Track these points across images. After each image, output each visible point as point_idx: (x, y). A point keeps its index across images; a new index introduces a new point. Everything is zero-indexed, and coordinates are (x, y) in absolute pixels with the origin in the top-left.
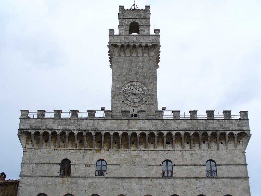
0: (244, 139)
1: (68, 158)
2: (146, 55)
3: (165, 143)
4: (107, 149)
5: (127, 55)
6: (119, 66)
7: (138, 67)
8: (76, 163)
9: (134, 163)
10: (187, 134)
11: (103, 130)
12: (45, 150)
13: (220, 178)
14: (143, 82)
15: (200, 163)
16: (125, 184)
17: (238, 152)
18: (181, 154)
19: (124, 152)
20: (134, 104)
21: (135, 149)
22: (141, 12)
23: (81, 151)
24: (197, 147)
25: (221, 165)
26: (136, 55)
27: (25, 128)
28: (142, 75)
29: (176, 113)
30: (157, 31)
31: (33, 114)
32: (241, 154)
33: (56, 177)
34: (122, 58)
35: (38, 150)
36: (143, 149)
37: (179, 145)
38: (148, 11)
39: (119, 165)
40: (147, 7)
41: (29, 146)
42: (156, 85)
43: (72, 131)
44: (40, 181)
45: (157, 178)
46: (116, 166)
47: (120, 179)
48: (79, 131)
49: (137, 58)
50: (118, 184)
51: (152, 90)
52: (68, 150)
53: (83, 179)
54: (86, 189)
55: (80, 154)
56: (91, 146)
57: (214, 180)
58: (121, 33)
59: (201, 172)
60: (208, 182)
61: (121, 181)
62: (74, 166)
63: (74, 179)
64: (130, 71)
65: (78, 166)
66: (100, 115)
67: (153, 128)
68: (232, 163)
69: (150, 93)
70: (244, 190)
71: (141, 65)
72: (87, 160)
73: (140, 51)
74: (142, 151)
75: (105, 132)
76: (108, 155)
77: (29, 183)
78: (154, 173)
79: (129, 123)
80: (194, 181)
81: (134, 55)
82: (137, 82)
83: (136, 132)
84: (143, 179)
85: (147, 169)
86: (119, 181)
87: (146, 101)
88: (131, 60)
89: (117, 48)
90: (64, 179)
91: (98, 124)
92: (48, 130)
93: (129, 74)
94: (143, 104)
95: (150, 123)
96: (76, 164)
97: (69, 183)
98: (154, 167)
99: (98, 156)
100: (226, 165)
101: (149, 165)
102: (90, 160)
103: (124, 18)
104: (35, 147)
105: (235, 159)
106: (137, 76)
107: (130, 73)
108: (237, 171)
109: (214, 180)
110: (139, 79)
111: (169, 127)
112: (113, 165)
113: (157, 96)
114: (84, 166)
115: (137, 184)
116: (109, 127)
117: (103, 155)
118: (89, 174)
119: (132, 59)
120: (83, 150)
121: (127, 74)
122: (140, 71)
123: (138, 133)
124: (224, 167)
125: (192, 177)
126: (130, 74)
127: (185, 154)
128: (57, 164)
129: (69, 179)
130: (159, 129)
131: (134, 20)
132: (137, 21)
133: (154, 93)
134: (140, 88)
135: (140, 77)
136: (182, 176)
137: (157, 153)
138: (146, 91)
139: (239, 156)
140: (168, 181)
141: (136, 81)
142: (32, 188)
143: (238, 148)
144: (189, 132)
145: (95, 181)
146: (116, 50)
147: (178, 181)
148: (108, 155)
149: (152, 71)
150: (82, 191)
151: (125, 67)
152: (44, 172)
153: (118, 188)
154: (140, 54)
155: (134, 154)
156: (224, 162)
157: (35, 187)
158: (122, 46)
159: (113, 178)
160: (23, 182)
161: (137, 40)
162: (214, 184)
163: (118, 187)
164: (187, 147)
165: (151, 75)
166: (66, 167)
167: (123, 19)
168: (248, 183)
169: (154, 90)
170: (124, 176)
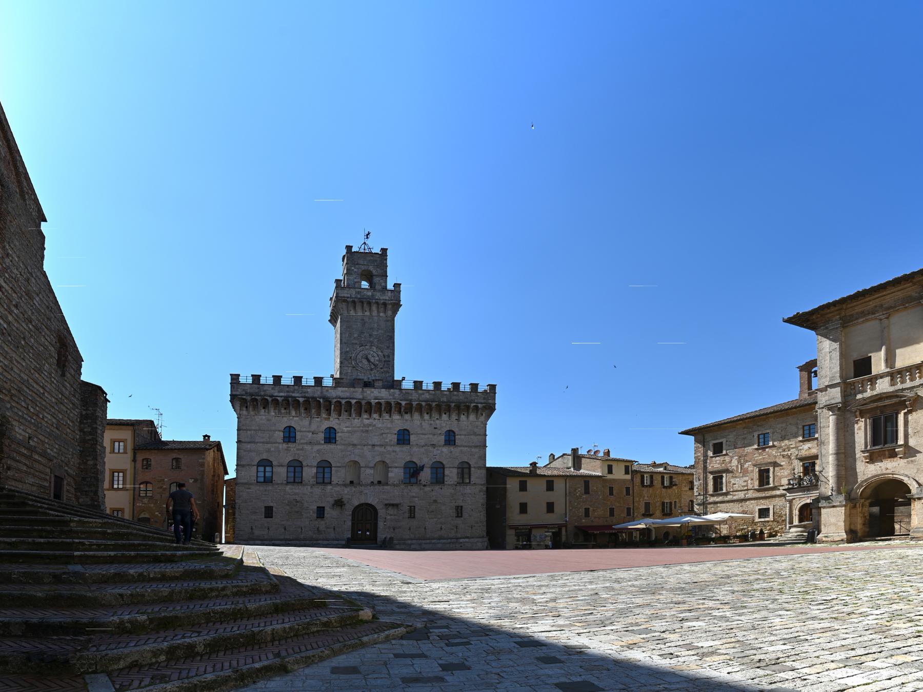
2: (381, 314)
27: (238, 393)
29: (418, 384)
30: (397, 286)
31: (246, 379)
40: (384, 251)
41: (245, 412)
51: (388, 356)
55: (306, 422)
56: (319, 414)
57: (452, 448)
60: (445, 450)
66: (327, 382)
72: (314, 427)
80: (431, 448)
86: (350, 448)
99: (326, 425)
104: (252, 413)
105: (476, 430)
117: (333, 422)
131: (366, 267)
140: (406, 448)
147: (415, 449)
154: (375, 313)
156: (463, 433)
158: (354, 302)
161: (373, 295)
164: (426, 417)
166: (290, 435)
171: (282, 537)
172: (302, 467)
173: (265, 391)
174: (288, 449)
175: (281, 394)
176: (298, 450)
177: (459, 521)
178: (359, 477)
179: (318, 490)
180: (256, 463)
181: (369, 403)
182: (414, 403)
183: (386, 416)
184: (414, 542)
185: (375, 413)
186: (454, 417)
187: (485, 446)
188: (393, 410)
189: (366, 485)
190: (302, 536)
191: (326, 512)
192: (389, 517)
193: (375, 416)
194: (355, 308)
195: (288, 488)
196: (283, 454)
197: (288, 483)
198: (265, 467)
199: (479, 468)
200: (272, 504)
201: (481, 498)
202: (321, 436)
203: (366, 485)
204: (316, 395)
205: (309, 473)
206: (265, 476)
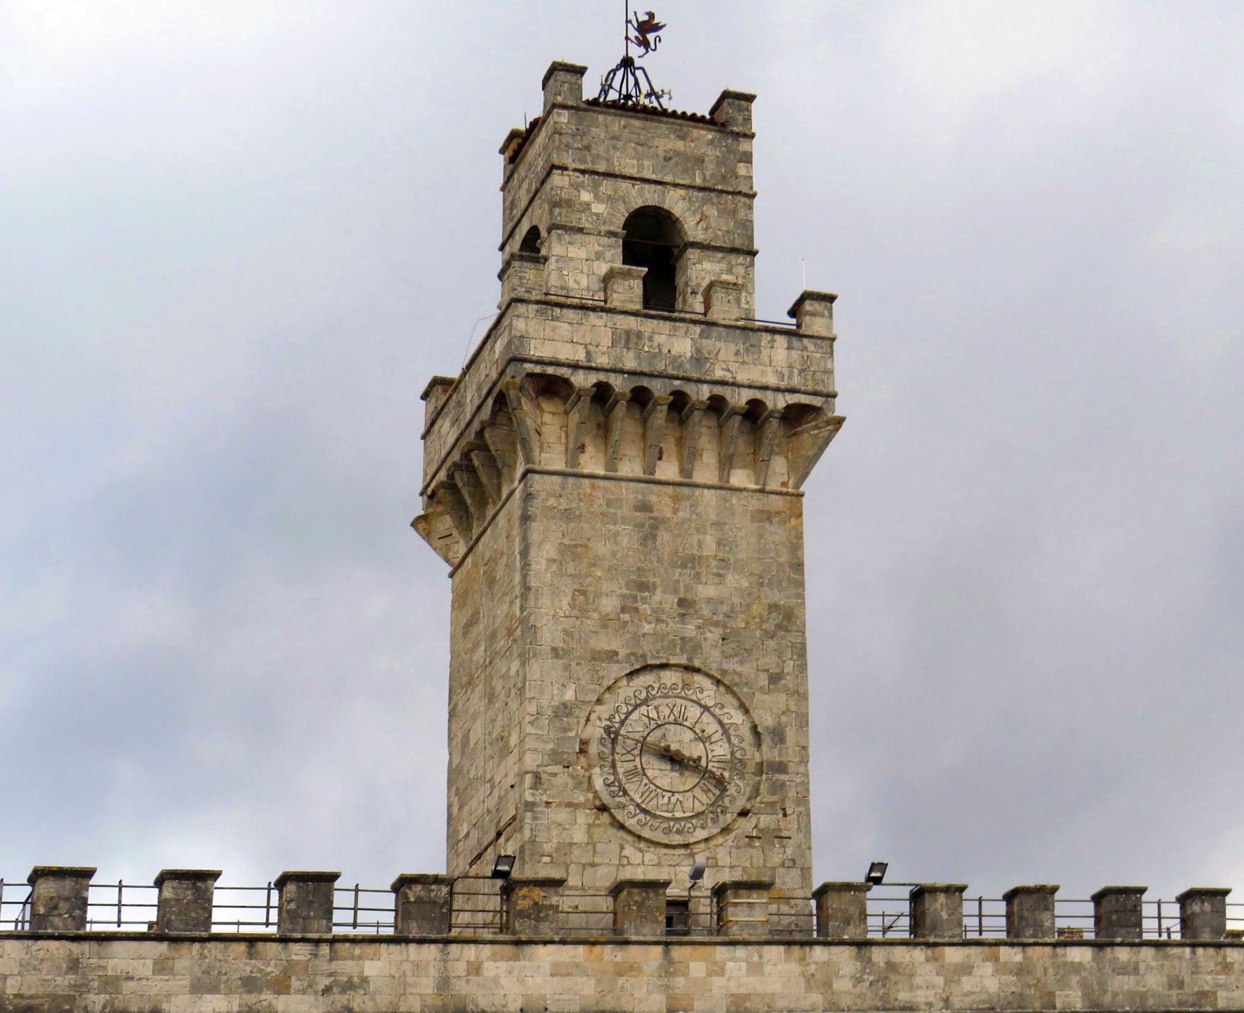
6: (576, 546)
7: (693, 558)
14: (724, 672)
22: (696, 133)
26: (682, 471)
28: (717, 624)
34: (586, 482)
38: (745, 136)
42: (803, 697)
49: (686, 490)
51: (779, 736)
58: (571, 284)
64: (644, 587)
69: (769, 753)
71: (714, 546)
81: (668, 470)
82: (689, 669)
88: (645, 507)
89: (558, 402)
91: (473, 978)
93: (636, 609)
103: (589, 166)
106: (690, 630)
107: (644, 600)
110: (697, 648)
113: (806, 775)
116: (543, 998)
119: (653, 499)
121: (623, 610)
122: (706, 591)
126: (645, 608)
132: (675, 202)
133: (791, 756)
134: (707, 718)
135: (708, 635)
138: (742, 740)
141: (683, 660)
146: (547, 418)
149: (774, 596)
151: (614, 554)
154: (706, 472)
165: (769, 626)
167: (583, 172)
169: (790, 734)
173: (110, 984)
194: (605, 430)
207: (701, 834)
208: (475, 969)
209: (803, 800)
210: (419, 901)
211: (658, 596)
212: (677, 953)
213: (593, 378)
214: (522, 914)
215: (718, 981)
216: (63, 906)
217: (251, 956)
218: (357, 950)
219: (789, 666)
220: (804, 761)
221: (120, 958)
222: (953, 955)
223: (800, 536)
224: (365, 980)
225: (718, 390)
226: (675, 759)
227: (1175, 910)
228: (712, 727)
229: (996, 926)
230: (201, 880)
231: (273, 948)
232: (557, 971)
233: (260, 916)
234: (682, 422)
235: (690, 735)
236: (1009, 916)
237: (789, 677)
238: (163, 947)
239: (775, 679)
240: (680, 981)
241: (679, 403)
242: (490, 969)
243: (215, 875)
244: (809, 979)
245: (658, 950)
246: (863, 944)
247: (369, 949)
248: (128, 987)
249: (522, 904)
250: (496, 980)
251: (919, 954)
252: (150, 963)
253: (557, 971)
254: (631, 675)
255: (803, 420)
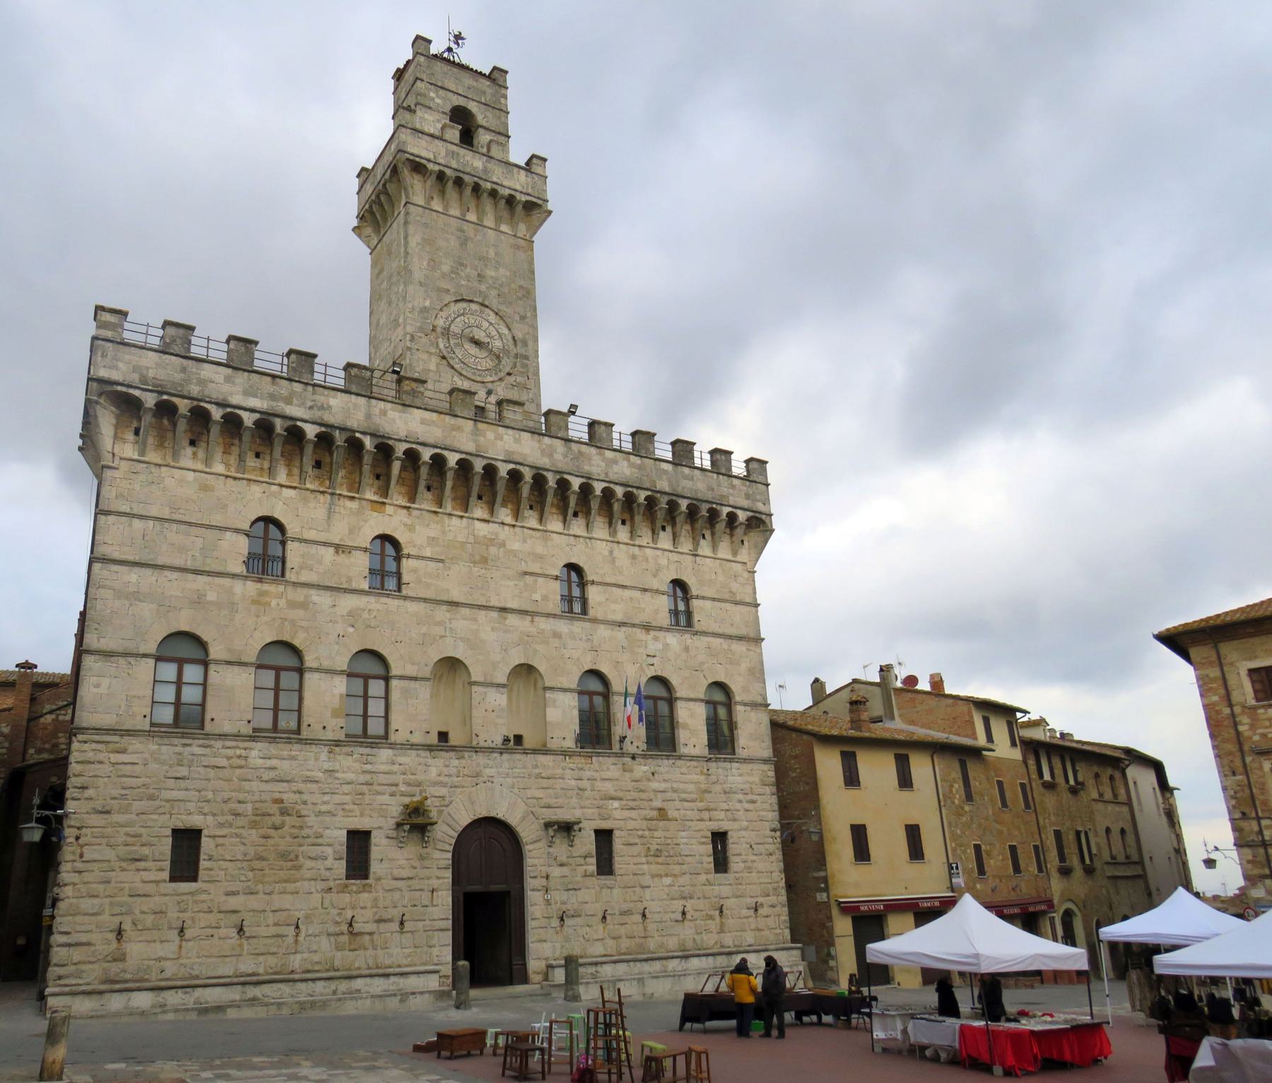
0: (754, 536)
1: (276, 516)
3: (570, 512)
4: (404, 504)
5: (452, 212)
8: (305, 537)
9: (484, 560)
10: (629, 499)
11: (400, 440)
12: (190, 476)
13: (704, 633)
15: (655, 584)
16: (461, 622)
17: (738, 567)
18: (606, 553)
19: (455, 521)
20: (474, 374)
21: (486, 516)
23: (321, 497)
24: (646, 539)
25: (703, 598)
32: (746, 575)
33: (234, 576)
35: (164, 469)
36: (509, 520)
37: (601, 525)
39: (442, 561)
42: (535, 328)
43: (299, 423)
44: (174, 585)
45: (548, 615)
46: (432, 565)
47: (445, 607)
48: (323, 429)
50: (440, 624)
51: (525, 344)
52: (274, 488)
53: (329, 593)
54: (339, 628)
55: (317, 508)
56: (356, 486)
59: (656, 612)
60: (673, 640)
61: (448, 615)
62: (296, 544)
63: (299, 590)
64: (461, 264)
65: (313, 549)
67: (544, 462)
68: (727, 596)
69: (520, 350)
70: (751, 671)
72: (338, 533)
73: (488, 204)
74: (506, 528)
75: (405, 446)
76: (405, 525)
77: (131, 590)
78: (539, 599)
79: (476, 432)
80: (640, 634)
81: (472, 217)
82: (482, 304)
83: (499, 464)
84: (509, 615)
85: (522, 583)
86: (442, 613)
87: (509, 374)
90: (266, 587)
92: (210, 402)
94: (501, 379)
95: (535, 444)
96: (306, 541)
97: (283, 602)
98: (540, 580)
99: (376, 523)
100: (714, 600)
101: (526, 573)
102: (351, 531)
104: (153, 456)
105: (735, 586)
106: (483, 287)
108: (735, 618)
109: (687, 636)
110: (486, 297)
111: (587, 468)
112: (423, 558)
114: (331, 550)
115: (493, 629)
117: (393, 520)
118: (349, 580)
120: (329, 497)
122: (490, 273)
123: (503, 469)
124: (708, 604)
125: (637, 622)
127: (616, 553)
128: (237, 531)
129: (281, 588)
130: (561, 466)
132: (473, 107)
136: (611, 617)
137: (546, 539)
139: (740, 579)
140: (578, 627)
142: (146, 610)
143: (739, 558)
144: (635, 491)
145: (370, 607)
147: (603, 632)
148: (405, 525)
149: (522, 282)
150: (327, 634)
152: (190, 553)
153: (442, 637)
155: (481, 534)
156: (709, 592)
157: (154, 606)
159: (425, 600)
160: (108, 583)
161: (485, 170)
162: (687, 649)
163: (438, 630)
164: (623, 533)
165: (520, 294)
166: (268, 547)
168: (761, 654)
169: (530, 344)
170: (455, 600)
171: (226, 969)
172: (300, 671)
173: (202, 382)
174: (259, 602)
175: (254, 402)
176: (292, 605)
177: (722, 886)
178: (467, 719)
179: (349, 764)
180: (151, 647)
181: (490, 471)
182: (598, 487)
183: (531, 519)
184: (622, 968)
185: (504, 505)
186: (686, 546)
187: (758, 640)
188: (550, 498)
189: (492, 750)
190: (296, 962)
191: (375, 852)
192: (556, 872)
193: (505, 514)
195: (257, 753)
196: (241, 621)
197: (256, 735)
198: (181, 662)
199: (754, 705)
200: (195, 821)
201: (766, 808)
202: (360, 564)
203: (492, 750)
204: (352, 423)
205: (325, 695)
206: (178, 704)
207: (489, 379)
208: (384, 413)
209: (537, 374)
210: (356, 376)
211: (468, 270)
212: (480, 425)
213: (437, 168)
214: (407, 393)
215: (499, 443)
216: (179, 341)
217: (273, 384)
218: (326, 392)
219: (529, 314)
220: (537, 357)
221: (207, 371)
222: (609, 454)
223: (533, 259)
224: (330, 407)
225: (495, 186)
226: (477, 343)
227: (708, 457)
228: (494, 333)
229: (628, 446)
230: (249, 343)
231: (285, 383)
232: (423, 422)
233: (279, 367)
234: (478, 198)
235: (483, 334)
236: (633, 443)
237: (529, 317)
238: (229, 371)
239: (523, 318)
240: (482, 439)
241: (476, 189)
242: (391, 414)
243: (256, 343)
244: (543, 451)
245: (471, 423)
246: (568, 440)
247: (332, 393)
248: (211, 386)
249: (406, 388)
250: (394, 420)
251: (593, 450)
252: (222, 377)
253: (423, 422)
254: (456, 301)
255: (531, 209)
